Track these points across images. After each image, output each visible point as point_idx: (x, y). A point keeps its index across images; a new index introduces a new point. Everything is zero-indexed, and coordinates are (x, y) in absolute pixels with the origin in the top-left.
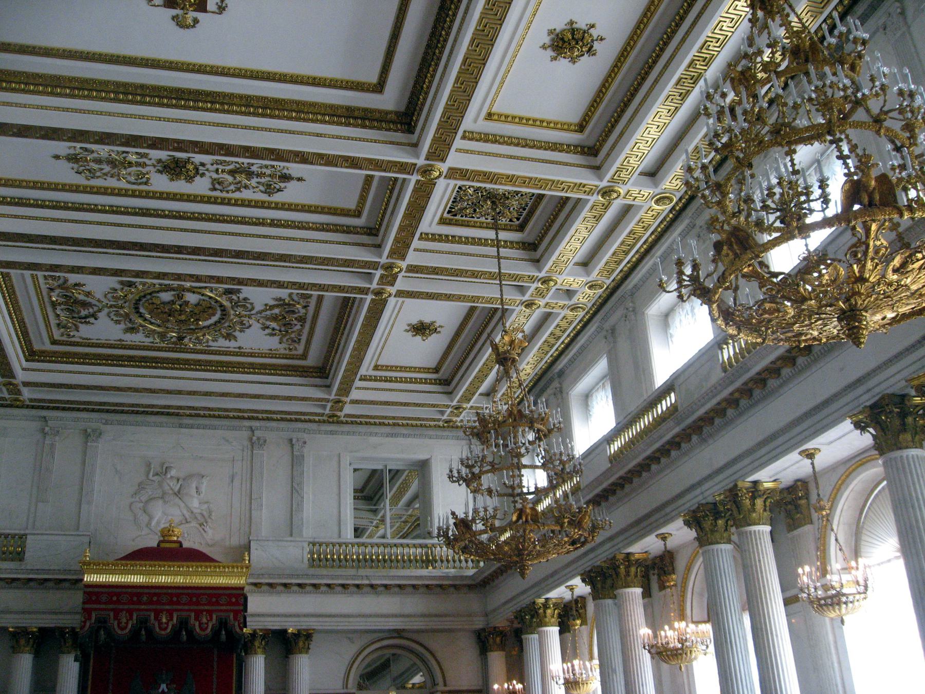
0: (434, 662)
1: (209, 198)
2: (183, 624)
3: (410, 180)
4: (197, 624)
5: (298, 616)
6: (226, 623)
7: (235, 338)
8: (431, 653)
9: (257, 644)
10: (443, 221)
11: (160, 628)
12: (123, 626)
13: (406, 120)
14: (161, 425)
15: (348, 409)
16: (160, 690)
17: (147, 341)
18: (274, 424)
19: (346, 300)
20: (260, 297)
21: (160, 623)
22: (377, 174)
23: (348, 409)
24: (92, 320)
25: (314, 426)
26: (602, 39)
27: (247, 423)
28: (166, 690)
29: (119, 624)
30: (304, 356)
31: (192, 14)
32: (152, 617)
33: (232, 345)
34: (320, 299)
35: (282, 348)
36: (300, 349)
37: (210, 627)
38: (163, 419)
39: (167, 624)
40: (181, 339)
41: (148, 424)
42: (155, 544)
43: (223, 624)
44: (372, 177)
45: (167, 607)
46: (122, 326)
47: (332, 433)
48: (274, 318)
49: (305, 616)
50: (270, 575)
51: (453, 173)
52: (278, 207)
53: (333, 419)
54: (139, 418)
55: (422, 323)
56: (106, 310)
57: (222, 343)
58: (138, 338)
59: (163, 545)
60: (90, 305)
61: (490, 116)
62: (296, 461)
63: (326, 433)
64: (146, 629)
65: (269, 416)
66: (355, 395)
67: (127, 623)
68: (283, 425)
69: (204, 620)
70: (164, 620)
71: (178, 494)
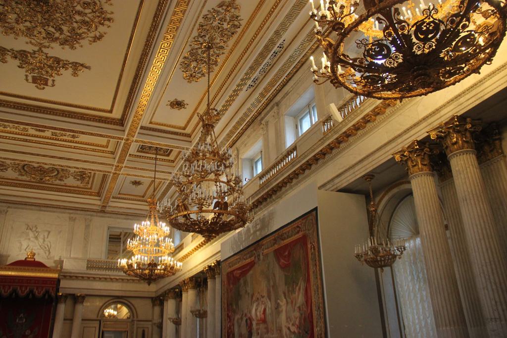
0: (133, 308)
1: (51, 138)
2: (31, 291)
3: (121, 142)
4: (37, 292)
6: (48, 292)
7: (63, 181)
8: (133, 306)
10: (138, 151)
13: (121, 122)
14: (32, 210)
15: (108, 209)
17: (28, 179)
18: (79, 212)
19: (104, 175)
20: (72, 170)
22: (111, 140)
23: (108, 209)
24: (5, 170)
25: (95, 214)
26: (187, 105)
27: (67, 211)
30: (91, 188)
31: (42, 86)
32: (19, 288)
33: (62, 183)
34: (95, 174)
35: (81, 185)
36: (89, 186)
38: (33, 207)
40: (41, 179)
41: (26, 209)
42: (24, 259)
44: (110, 140)
45: (25, 284)
46: (18, 173)
47: (102, 217)
48: (78, 175)
50: (71, 273)
51: (136, 141)
52: (77, 142)
53: (103, 212)
54: (23, 206)
55: (135, 181)
56: (11, 168)
57: (58, 182)
58: (24, 178)
59: (28, 259)
60: (5, 166)
61: (151, 123)
62: (87, 227)
63: (99, 216)
65: (76, 209)
66: (110, 204)
68: (82, 212)
70: (23, 289)
71: (36, 238)
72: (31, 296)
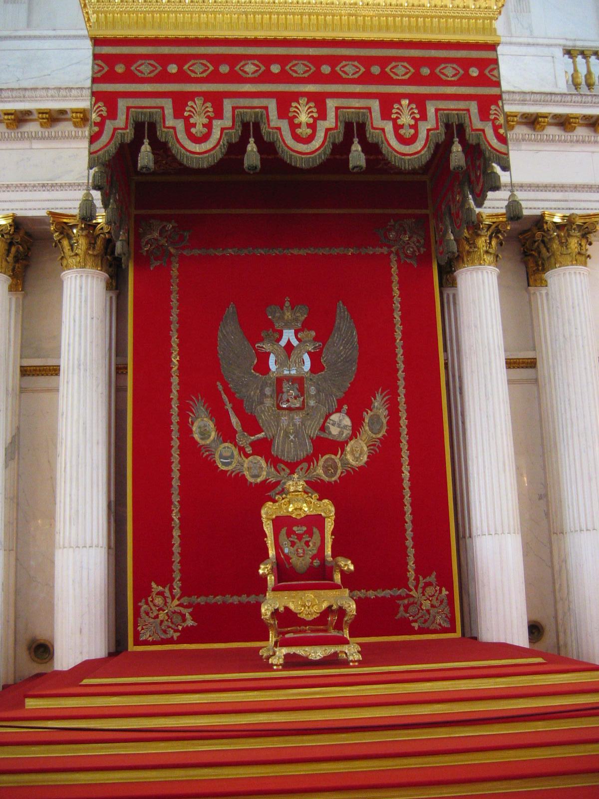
4: (389, 126)
5: (562, 188)
6: (461, 128)
9: (481, 242)
11: (297, 138)
12: (199, 139)
16: (283, 343)
21: (294, 126)
28: (295, 342)
29: (188, 126)
37: (422, 135)
39: (313, 126)
43: (455, 129)
49: (576, 188)
64: (259, 141)
67: (209, 126)
69: (406, 119)
70: (304, 118)
72: (357, 156)
